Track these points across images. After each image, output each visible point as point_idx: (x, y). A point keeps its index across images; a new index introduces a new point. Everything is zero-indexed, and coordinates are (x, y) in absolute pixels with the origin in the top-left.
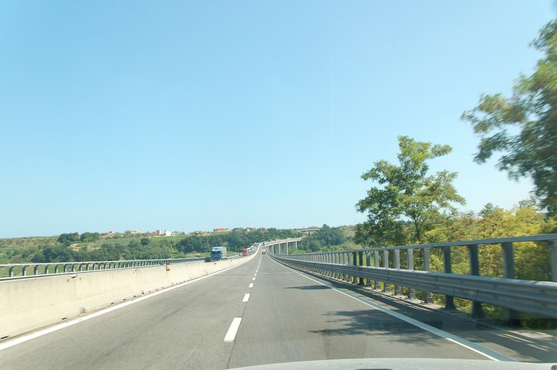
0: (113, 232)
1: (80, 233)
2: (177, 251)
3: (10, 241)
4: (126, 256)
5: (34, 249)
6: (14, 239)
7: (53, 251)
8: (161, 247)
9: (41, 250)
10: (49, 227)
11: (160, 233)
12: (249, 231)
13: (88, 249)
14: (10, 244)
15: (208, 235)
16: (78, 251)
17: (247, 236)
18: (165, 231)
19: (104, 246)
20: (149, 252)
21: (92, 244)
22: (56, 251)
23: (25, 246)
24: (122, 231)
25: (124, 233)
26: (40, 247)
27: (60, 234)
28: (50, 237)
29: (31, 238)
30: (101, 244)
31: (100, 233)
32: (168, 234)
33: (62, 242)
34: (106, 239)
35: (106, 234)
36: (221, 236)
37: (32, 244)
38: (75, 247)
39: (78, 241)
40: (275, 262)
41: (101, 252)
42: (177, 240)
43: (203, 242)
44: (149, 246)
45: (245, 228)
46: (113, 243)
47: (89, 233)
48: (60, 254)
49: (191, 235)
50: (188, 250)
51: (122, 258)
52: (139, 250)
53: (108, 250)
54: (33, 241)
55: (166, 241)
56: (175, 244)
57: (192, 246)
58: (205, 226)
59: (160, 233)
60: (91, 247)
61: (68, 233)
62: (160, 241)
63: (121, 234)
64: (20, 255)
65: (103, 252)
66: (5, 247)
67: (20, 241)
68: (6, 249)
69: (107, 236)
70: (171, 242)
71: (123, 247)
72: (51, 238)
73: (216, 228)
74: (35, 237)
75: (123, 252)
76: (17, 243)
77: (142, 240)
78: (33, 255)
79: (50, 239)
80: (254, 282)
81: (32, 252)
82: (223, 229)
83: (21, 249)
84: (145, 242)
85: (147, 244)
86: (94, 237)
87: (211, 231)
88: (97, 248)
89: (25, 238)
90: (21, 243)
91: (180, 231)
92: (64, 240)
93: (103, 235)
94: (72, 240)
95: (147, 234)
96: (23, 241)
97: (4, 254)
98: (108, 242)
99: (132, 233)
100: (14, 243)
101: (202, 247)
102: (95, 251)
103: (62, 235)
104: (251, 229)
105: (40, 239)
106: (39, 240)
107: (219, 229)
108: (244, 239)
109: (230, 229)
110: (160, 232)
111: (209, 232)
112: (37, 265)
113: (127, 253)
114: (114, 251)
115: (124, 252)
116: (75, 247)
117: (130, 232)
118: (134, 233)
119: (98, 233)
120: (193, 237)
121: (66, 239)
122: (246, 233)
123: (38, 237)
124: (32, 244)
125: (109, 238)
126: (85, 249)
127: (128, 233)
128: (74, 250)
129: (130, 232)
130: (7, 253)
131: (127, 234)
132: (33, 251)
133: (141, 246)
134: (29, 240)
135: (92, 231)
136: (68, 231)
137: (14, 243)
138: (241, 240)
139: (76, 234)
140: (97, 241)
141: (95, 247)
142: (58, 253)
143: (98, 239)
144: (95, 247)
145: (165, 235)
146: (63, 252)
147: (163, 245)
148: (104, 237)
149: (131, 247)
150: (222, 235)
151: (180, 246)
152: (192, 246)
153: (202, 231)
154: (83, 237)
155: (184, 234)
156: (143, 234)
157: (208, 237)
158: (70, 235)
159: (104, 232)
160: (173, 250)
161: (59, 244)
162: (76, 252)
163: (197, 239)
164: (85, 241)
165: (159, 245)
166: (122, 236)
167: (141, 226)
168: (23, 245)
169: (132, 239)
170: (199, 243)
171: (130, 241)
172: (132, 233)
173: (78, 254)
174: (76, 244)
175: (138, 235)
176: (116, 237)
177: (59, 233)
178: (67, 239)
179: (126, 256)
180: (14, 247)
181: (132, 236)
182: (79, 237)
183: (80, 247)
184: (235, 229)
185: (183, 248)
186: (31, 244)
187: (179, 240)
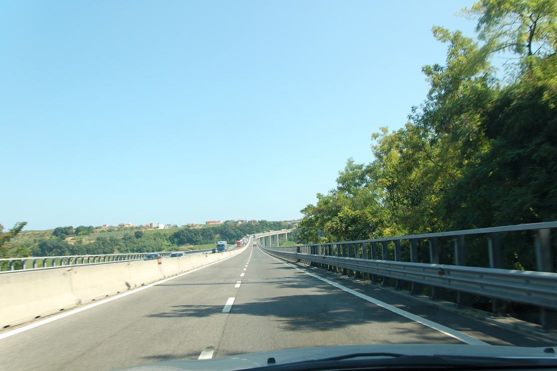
0: (107, 226)
1: (75, 227)
2: (170, 243)
4: (120, 248)
5: (29, 243)
7: (49, 245)
8: (155, 239)
9: (37, 244)
11: (153, 227)
12: (240, 223)
15: (201, 227)
16: (73, 244)
17: (238, 228)
18: (158, 224)
19: (98, 239)
20: (143, 245)
21: (87, 237)
22: (51, 244)
23: (20, 240)
24: (116, 224)
25: (118, 226)
26: (35, 241)
27: (55, 228)
30: (96, 237)
31: (94, 226)
32: (162, 227)
33: (57, 236)
34: (100, 232)
36: (213, 229)
37: (27, 238)
38: (70, 240)
40: (264, 253)
41: (96, 245)
42: (170, 233)
43: (195, 234)
44: (143, 239)
45: (236, 221)
46: (107, 236)
47: (83, 227)
48: (59, 247)
49: (183, 228)
50: (181, 243)
51: (117, 250)
52: (133, 242)
53: (103, 243)
54: (28, 235)
55: (159, 234)
56: (168, 237)
57: (185, 239)
59: (153, 227)
60: (86, 241)
61: (63, 226)
62: (154, 234)
63: (115, 227)
65: (97, 245)
69: (101, 230)
70: (165, 235)
72: (46, 232)
73: (208, 221)
74: (30, 231)
75: (117, 245)
77: (136, 233)
80: (245, 272)
82: (215, 222)
83: (17, 243)
84: (138, 235)
86: (89, 230)
87: (203, 224)
91: (173, 223)
92: (59, 233)
93: (97, 228)
94: (67, 234)
95: (141, 227)
98: (103, 235)
99: (125, 226)
101: (195, 239)
104: (242, 221)
105: (35, 233)
107: (211, 222)
108: (236, 232)
109: (222, 221)
110: (153, 225)
111: (201, 225)
112: (46, 259)
113: (121, 246)
114: (109, 244)
115: (119, 245)
117: (124, 225)
118: (127, 226)
119: (92, 227)
120: (186, 229)
121: (61, 233)
122: (238, 225)
123: (32, 231)
124: (27, 238)
125: (103, 231)
126: (80, 242)
128: (69, 243)
131: (121, 227)
132: (29, 244)
133: (135, 239)
135: (87, 225)
136: (63, 225)
138: (232, 232)
139: (70, 228)
140: (92, 234)
141: (90, 240)
144: (90, 240)
145: (158, 227)
146: (59, 245)
147: (157, 238)
148: (98, 230)
150: (214, 228)
151: (173, 238)
152: (185, 239)
153: (195, 223)
154: (78, 231)
155: (176, 226)
156: (136, 228)
158: (65, 228)
160: (166, 243)
161: (54, 237)
162: (71, 245)
163: (190, 231)
164: (80, 235)
165: (152, 238)
166: (116, 229)
167: (134, 218)
168: (18, 239)
169: (126, 232)
170: (192, 236)
171: (124, 234)
172: (125, 226)
173: (73, 247)
174: (71, 238)
175: (132, 228)
176: (110, 230)
177: (53, 227)
178: (62, 232)
179: (120, 248)
181: (126, 229)
182: (74, 231)
183: (75, 241)
184: (226, 222)
185: (176, 240)
186: (26, 238)
187: (172, 232)
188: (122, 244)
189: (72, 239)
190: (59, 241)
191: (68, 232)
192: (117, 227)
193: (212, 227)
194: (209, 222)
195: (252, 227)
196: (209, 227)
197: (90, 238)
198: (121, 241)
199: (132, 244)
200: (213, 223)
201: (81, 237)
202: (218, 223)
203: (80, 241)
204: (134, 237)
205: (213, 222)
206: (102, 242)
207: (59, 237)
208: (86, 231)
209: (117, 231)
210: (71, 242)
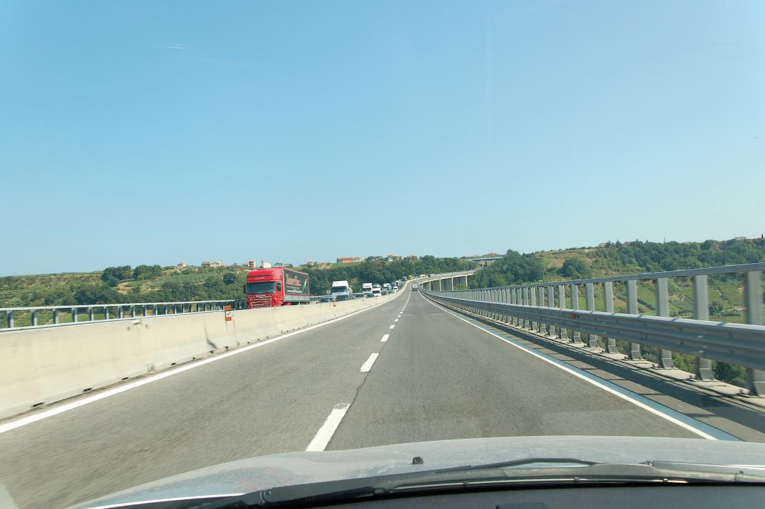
0: (184, 265)
1: (133, 267)
3: (31, 280)
5: (62, 291)
6: (38, 276)
7: (89, 294)
9: (74, 293)
10: (89, 260)
11: (255, 267)
12: (390, 260)
13: (141, 290)
14: (31, 284)
15: (328, 268)
17: (388, 268)
18: (262, 262)
19: (165, 286)
21: (149, 283)
23: (53, 286)
25: (200, 265)
26: (72, 289)
27: (103, 269)
28: (90, 273)
29: (63, 274)
30: (163, 282)
34: (172, 275)
35: (172, 268)
36: (348, 269)
39: (129, 278)
41: (160, 295)
43: (319, 278)
46: (180, 281)
48: (100, 295)
53: (172, 292)
54: (65, 279)
58: (326, 257)
59: (255, 267)
60: (146, 288)
61: (116, 266)
64: (43, 300)
65: (163, 294)
66: (23, 289)
67: (45, 280)
68: (24, 291)
69: (173, 271)
71: (195, 287)
72: (91, 275)
73: (340, 258)
74: (69, 274)
75: (195, 295)
76: (42, 283)
78: (60, 300)
79: (90, 276)
81: (59, 296)
82: (351, 259)
85: (233, 282)
86: (154, 271)
87: (332, 263)
88: (156, 289)
89: (55, 275)
90: (48, 282)
93: (167, 268)
95: (234, 267)
96: (51, 280)
97: (18, 299)
98: (172, 280)
100: (38, 282)
101: (318, 286)
102: (152, 293)
103: (107, 270)
104: (394, 258)
106: (74, 277)
108: (383, 274)
109: (363, 258)
110: (255, 263)
111: (328, 264)
113: (201, 296)
116: (123, 288)
117: (209, 265)
118: (214, 266)
119: (159, 267)
121: (114, 275)
123: (74, 273)
125: (176, 273)
126: (137, 290)
127: (206, 265)
128: (119, 292)
129: (209, 265)
130: (23, 298)
132: (62, 294)
133: (224, 287)
134: (60, 277)
135: (150, 263)
136: (116, 264)
137: (38, 282)
139: (127, 268)
140: (157, 279)
141: (153, 287)
142: (95, 296)
143: (159, 276)
144: (153, 287)
149: (208, 287)
150: (348, 268)
153: (320, 262)
154: (138, 272)
156: (228, 268)
157: (328, 270)
158: (119, 269)
159: (170, 265)
161: (101, 283)
162: (122, 295)
164: (140, 279)
166: (197, 270)
168: (50, 286)
169: (210, 274)
175: (220, 269)
176: (187, 272)
177: (102, 268)
178: (114, 275)
180: (37, 287)
181: (211, 270)
183: (130, 288)
184: (370, 258)
186: (62, 283)
188: (203, 293)
189: (126, 286)
190: (103, 288)
191: (124, 275)
192: (199, 268)
193: (346, 266)
194: (342, 260)
195: (410, 267)
196: (340, 266)
197: (154, 284)
198: (202, 289)
199: (220, 293)
200: (349, 261)
201: (139, 282)
202: (356, 261)
203: (137, 288)
204: (223, 283)
205: (347, 259)
206: (171, 290)
207: (108, 282)
208: (150, 272)
209: (198, 273)
210: (123, 290)
